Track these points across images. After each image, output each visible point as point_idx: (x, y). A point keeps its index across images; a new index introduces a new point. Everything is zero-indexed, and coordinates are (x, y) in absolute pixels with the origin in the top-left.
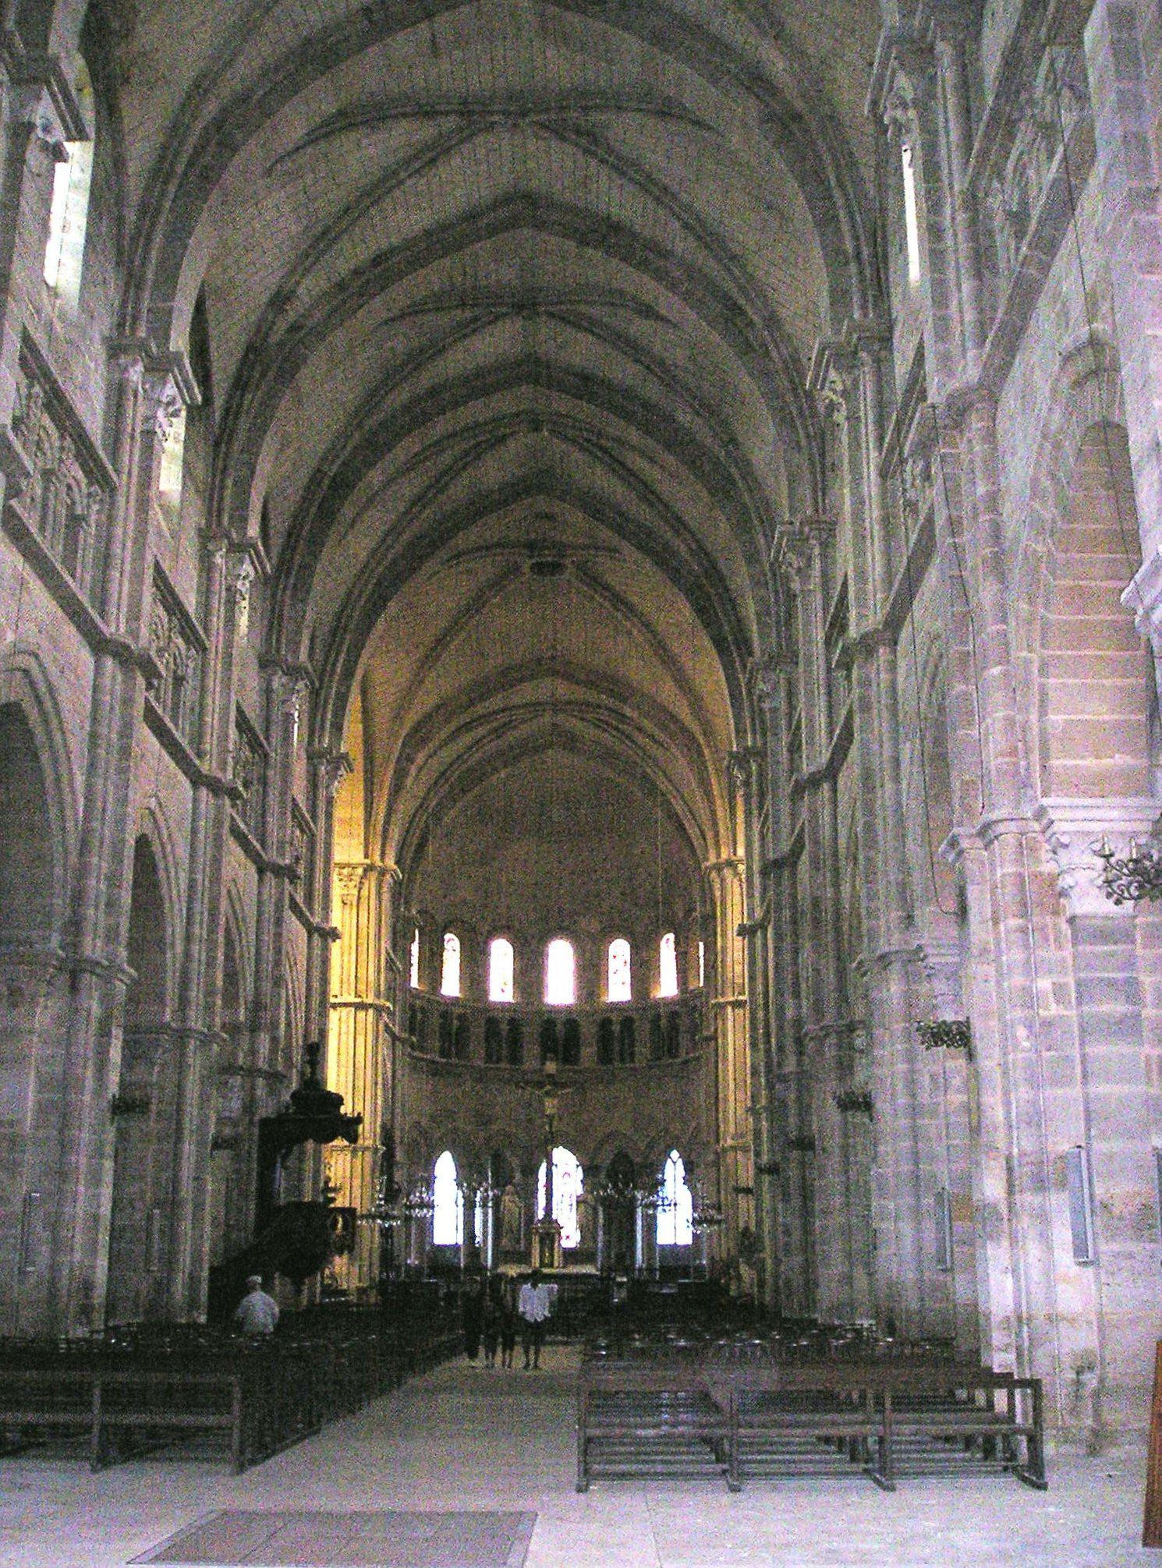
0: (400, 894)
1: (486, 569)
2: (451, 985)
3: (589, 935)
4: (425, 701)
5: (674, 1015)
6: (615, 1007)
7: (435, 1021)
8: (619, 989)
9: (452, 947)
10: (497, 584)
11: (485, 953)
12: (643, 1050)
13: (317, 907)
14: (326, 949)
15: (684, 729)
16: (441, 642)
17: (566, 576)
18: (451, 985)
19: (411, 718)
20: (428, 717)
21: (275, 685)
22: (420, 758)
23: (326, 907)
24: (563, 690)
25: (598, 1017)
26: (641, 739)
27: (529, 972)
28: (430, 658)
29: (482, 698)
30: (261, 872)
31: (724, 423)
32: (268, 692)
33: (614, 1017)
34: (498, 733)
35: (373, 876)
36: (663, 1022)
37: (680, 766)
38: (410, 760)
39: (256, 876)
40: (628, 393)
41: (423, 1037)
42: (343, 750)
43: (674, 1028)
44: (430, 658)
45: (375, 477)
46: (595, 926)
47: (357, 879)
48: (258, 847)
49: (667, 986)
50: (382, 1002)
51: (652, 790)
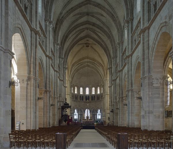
1: (81, 46)
2: (76, 92)
3: (90, 87)
4: (73, 62)
5: (99, 95)
6: (93, 94)
7: (74, 96)
8: (93, 93)
10: (82, 48)
11: (80, 89)
12: (96, 99)
13: (65, 84)
14: (65, 88)
15: (102, 65)
16: (76, 55)
18: (76, 92)
19: (72, 64)
21: (61, 60)
24: (88, 60)
26: (96, 66)
28: (74, 57)
29: (80, 61)
31: (110, 29)
32: (60, 61)
33: (93, 96)
34: (81, 65)
36: (98, 96)
37: (101, 69)
38: (72, 68)
40: (98, 25)
43: (99, 97)
44: (74, 57)
45: (70, 36)
46: (91, 86)
49: (99, 93)
51: (98, 72)
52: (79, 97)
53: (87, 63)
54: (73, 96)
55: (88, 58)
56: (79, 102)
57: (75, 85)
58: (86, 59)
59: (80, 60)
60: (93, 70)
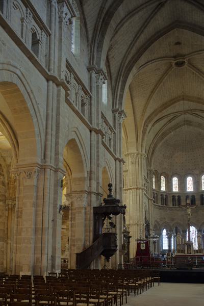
0: (149, 161)
2: (163, 189)
4: (149, 111)
7: (159, 197)
9: (163, 178)
10: (166, 73)
16: (152, 92)
17: (185, 66)
18: (163, 189)
20: (151, 114)
22: (150, 126)
23: (120, 153)
25: (200, 194)
27: (182, 184)
30: (91, 131)
32: (91, 78)
35: (139, 156)
39: (89, 133)
41: (157, 200)
42: (122, 109)
47: (135, 157)
48: (90, 124)
50: (143, 187)
52: (170, 199)
53: (182, 117)
54: (157, 196)
55: (184, 98)
56: (171, 209)
57: (160, 172)
58: (179, 101)
59: (165, 106)
60: (200, 130)
